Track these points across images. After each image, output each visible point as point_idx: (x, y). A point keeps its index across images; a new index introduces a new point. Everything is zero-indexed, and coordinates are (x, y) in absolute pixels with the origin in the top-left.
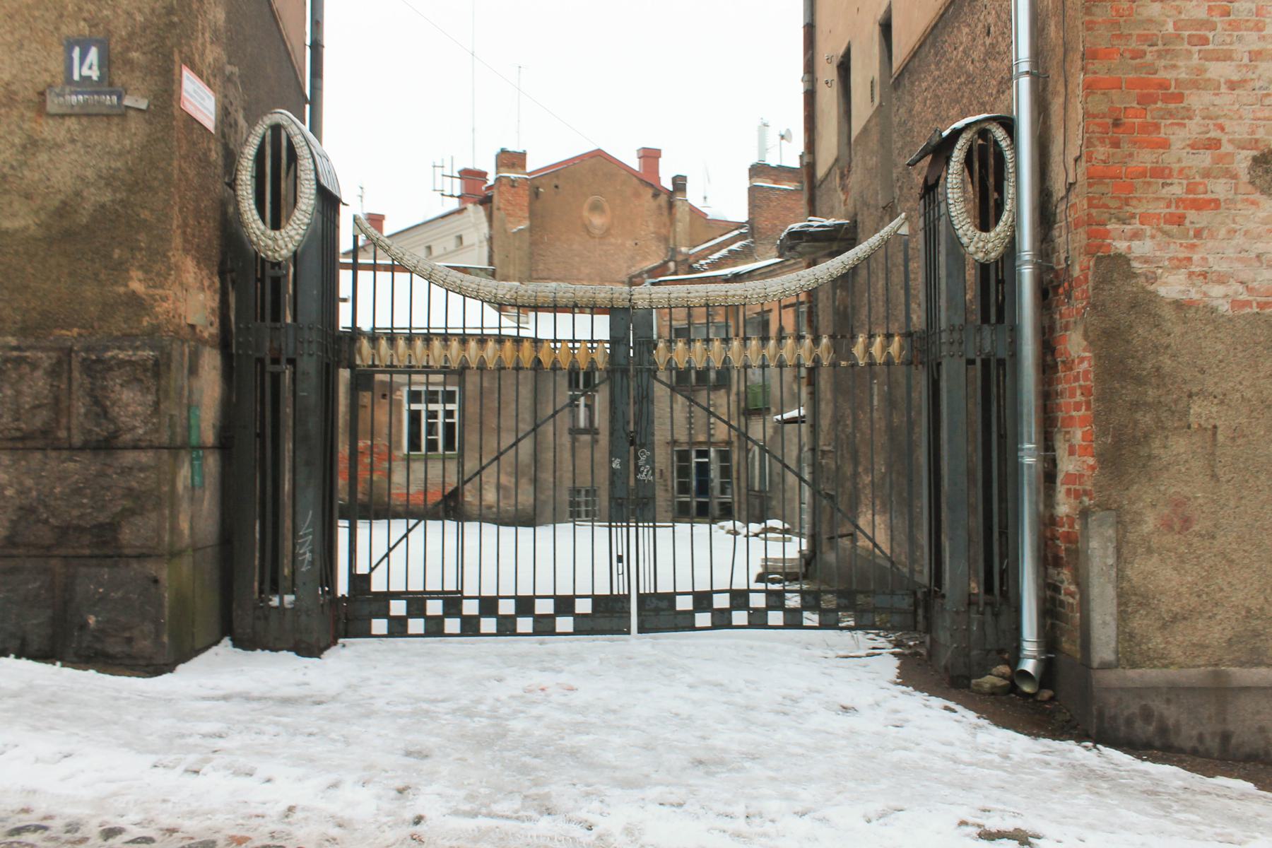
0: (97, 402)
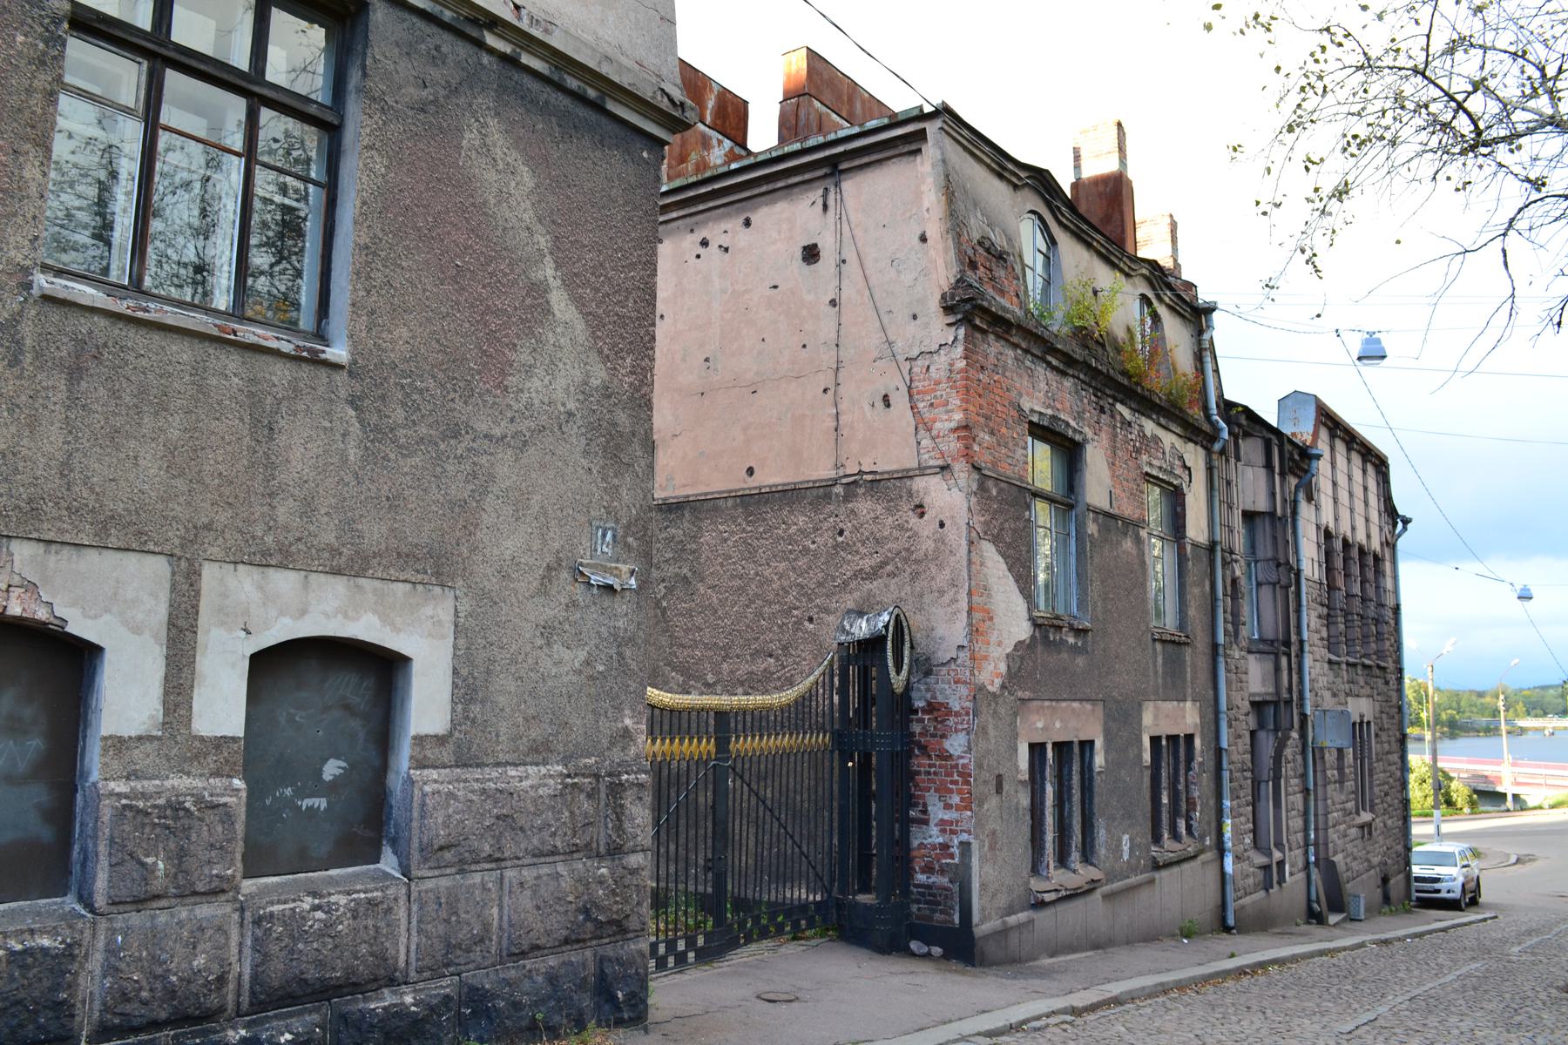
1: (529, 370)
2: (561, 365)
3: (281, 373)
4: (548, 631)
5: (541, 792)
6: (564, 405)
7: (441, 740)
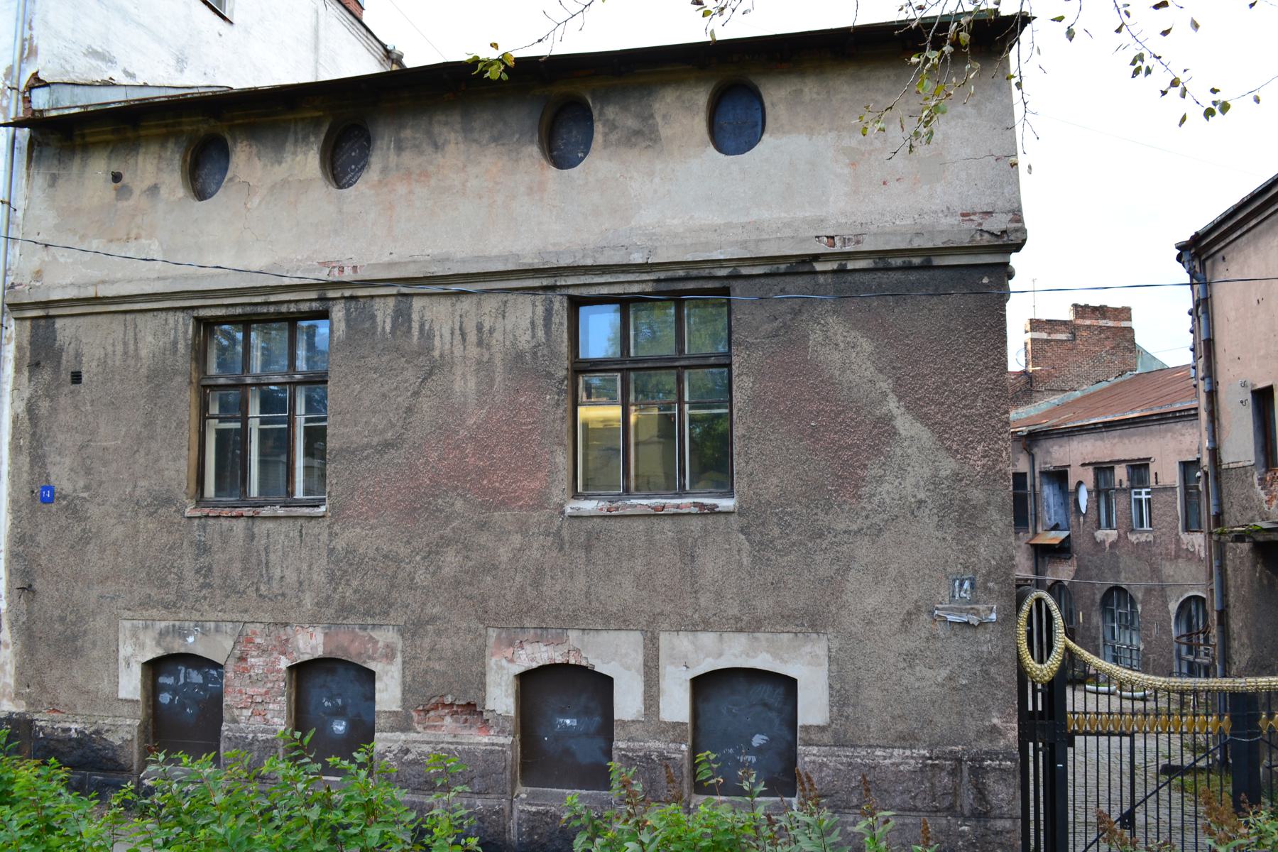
0: (980, 792)
1: (880, 480)
2: (909, 469)
3: (696, 525)
4: (910, 658)
5: (901, 768)
6: (914, 496)
7: (822, 729)
